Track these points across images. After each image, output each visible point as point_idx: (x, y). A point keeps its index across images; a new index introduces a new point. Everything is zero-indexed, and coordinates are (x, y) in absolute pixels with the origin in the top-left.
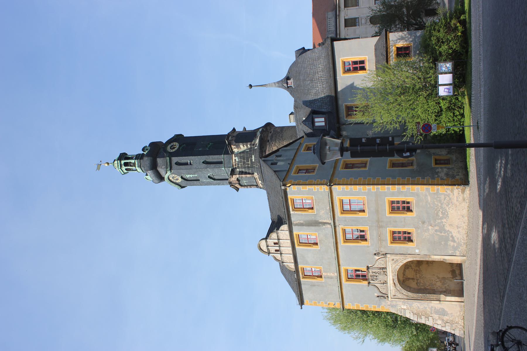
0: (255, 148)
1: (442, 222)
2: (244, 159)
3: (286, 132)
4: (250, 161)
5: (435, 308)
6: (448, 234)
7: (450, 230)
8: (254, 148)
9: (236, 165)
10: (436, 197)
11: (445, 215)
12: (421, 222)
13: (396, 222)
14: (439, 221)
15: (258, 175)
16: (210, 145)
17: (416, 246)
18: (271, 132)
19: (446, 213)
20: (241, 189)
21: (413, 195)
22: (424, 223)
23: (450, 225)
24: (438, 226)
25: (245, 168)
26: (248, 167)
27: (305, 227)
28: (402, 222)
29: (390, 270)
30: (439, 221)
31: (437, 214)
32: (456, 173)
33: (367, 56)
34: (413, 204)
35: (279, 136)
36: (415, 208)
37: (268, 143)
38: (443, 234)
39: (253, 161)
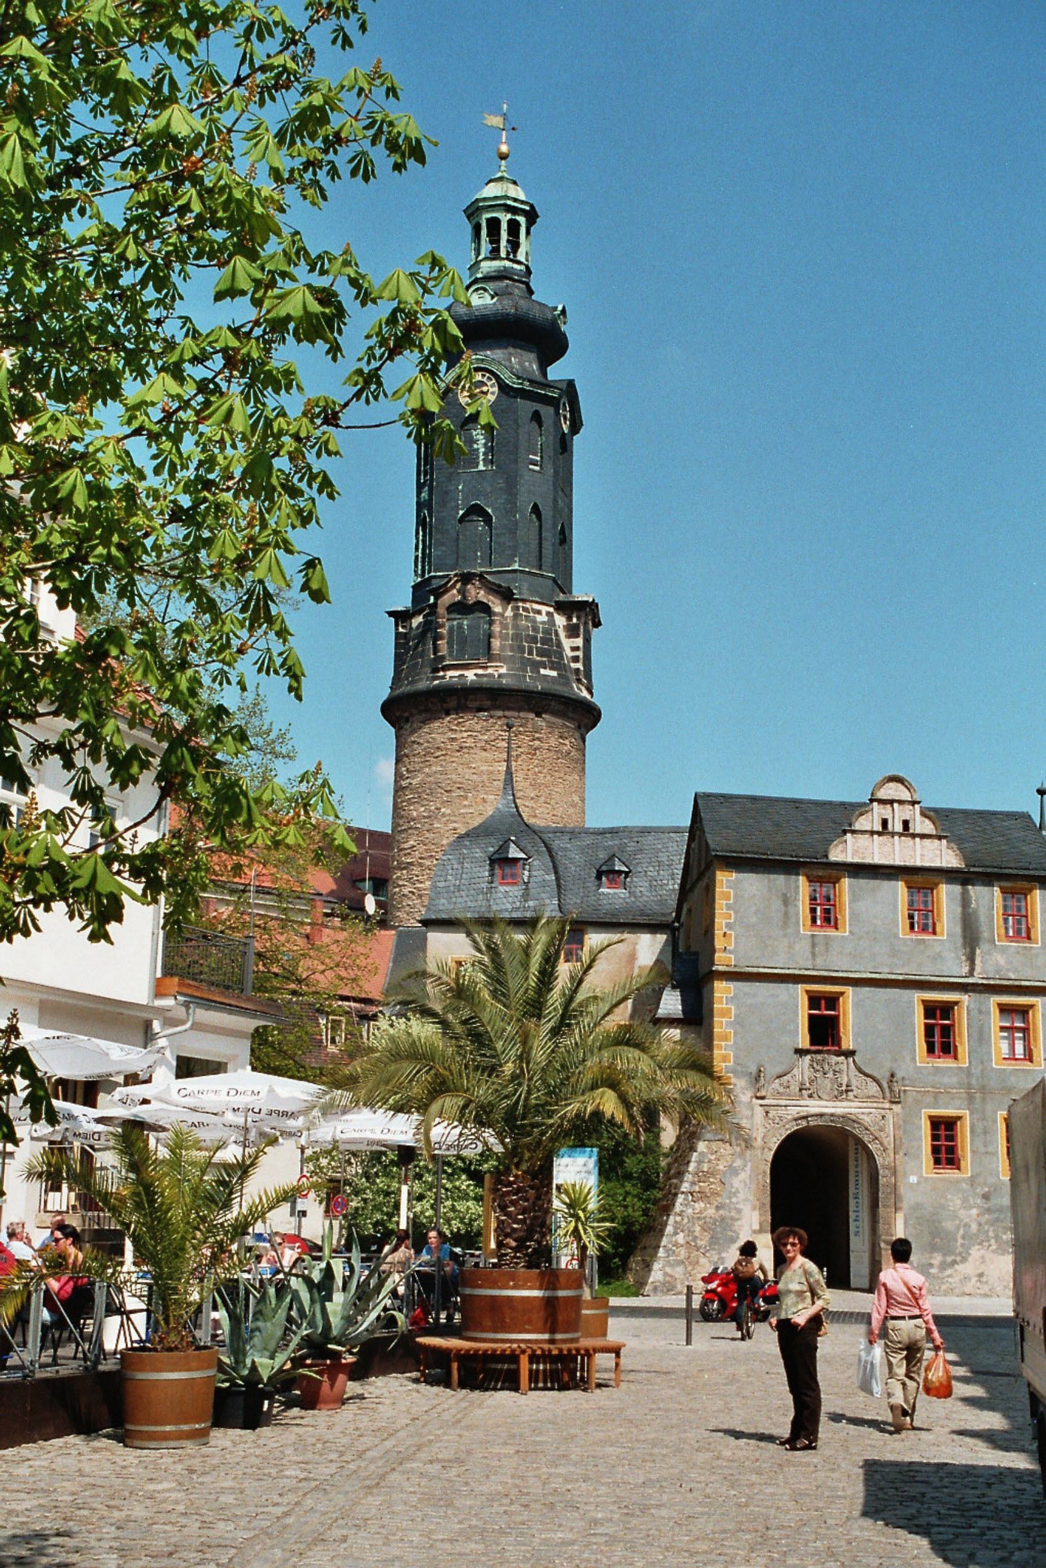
2: (544, 641)
4: (538, 658)
5: (738, 1219)
6: (960, 1254)
7: (970, 1259)
9: (525, 609)
13: (985, 1132)
14: (991, 1234)
17: (927, 1179)
22: (986, 1197)
23: (983, 1257)
24: (979, 1230)
27: (959, 910)
29: (853, 1111)
30: (991, 1234)
38: (960, 1241)
39: (543, 671)
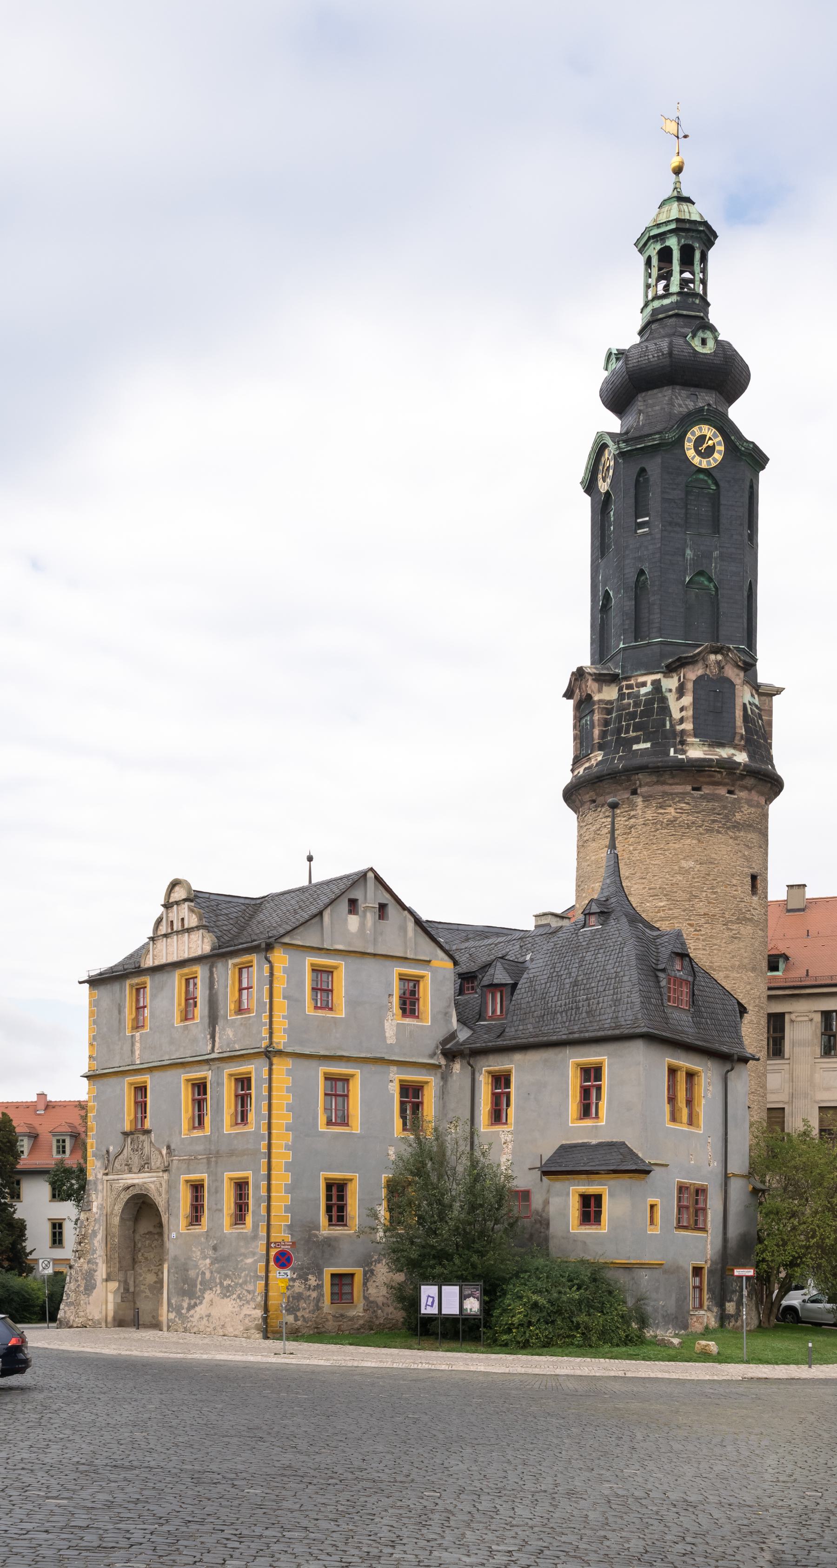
0: (672, 750)
1: (216, 1286)
3: (731, 841)
4: (635, 734)
8: (674, 746)
10: (252, 1274)
11: (227, 1292)
12: (216, 1244)
15: (597, 765)
16: (706, 583)
18: (730, 792)
19: (228, 1294)
20: (571, 703)
21: (256, 1227)
25: (619, 718)
26: (619, 731)
28: (216, 1204)
30: (218, 1281)
31: (227, 1276)
32: (303, 1316)
33: (604, 1123)
34: (242, 1228)
35: (714, 821)
36: (237, 1231)
37: (689, 788)
39: (635, 747)
